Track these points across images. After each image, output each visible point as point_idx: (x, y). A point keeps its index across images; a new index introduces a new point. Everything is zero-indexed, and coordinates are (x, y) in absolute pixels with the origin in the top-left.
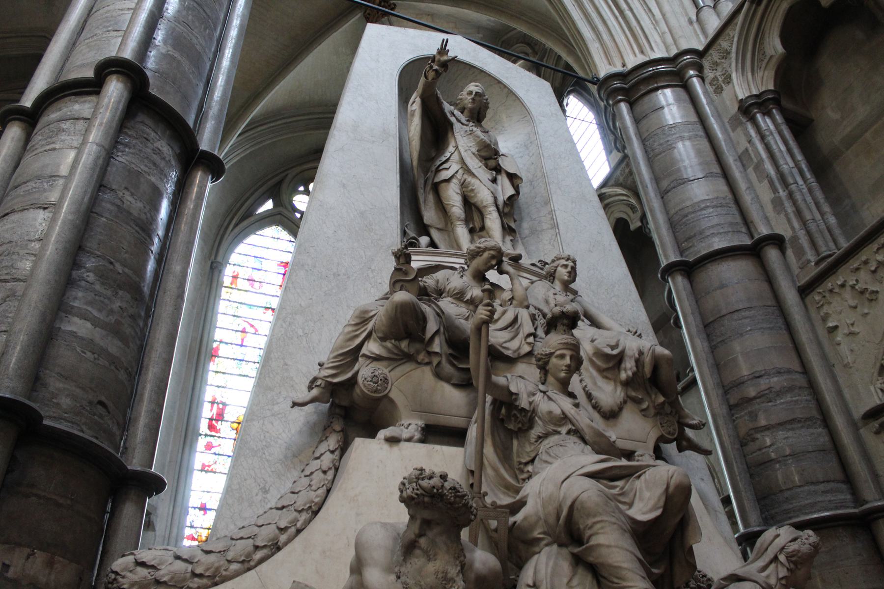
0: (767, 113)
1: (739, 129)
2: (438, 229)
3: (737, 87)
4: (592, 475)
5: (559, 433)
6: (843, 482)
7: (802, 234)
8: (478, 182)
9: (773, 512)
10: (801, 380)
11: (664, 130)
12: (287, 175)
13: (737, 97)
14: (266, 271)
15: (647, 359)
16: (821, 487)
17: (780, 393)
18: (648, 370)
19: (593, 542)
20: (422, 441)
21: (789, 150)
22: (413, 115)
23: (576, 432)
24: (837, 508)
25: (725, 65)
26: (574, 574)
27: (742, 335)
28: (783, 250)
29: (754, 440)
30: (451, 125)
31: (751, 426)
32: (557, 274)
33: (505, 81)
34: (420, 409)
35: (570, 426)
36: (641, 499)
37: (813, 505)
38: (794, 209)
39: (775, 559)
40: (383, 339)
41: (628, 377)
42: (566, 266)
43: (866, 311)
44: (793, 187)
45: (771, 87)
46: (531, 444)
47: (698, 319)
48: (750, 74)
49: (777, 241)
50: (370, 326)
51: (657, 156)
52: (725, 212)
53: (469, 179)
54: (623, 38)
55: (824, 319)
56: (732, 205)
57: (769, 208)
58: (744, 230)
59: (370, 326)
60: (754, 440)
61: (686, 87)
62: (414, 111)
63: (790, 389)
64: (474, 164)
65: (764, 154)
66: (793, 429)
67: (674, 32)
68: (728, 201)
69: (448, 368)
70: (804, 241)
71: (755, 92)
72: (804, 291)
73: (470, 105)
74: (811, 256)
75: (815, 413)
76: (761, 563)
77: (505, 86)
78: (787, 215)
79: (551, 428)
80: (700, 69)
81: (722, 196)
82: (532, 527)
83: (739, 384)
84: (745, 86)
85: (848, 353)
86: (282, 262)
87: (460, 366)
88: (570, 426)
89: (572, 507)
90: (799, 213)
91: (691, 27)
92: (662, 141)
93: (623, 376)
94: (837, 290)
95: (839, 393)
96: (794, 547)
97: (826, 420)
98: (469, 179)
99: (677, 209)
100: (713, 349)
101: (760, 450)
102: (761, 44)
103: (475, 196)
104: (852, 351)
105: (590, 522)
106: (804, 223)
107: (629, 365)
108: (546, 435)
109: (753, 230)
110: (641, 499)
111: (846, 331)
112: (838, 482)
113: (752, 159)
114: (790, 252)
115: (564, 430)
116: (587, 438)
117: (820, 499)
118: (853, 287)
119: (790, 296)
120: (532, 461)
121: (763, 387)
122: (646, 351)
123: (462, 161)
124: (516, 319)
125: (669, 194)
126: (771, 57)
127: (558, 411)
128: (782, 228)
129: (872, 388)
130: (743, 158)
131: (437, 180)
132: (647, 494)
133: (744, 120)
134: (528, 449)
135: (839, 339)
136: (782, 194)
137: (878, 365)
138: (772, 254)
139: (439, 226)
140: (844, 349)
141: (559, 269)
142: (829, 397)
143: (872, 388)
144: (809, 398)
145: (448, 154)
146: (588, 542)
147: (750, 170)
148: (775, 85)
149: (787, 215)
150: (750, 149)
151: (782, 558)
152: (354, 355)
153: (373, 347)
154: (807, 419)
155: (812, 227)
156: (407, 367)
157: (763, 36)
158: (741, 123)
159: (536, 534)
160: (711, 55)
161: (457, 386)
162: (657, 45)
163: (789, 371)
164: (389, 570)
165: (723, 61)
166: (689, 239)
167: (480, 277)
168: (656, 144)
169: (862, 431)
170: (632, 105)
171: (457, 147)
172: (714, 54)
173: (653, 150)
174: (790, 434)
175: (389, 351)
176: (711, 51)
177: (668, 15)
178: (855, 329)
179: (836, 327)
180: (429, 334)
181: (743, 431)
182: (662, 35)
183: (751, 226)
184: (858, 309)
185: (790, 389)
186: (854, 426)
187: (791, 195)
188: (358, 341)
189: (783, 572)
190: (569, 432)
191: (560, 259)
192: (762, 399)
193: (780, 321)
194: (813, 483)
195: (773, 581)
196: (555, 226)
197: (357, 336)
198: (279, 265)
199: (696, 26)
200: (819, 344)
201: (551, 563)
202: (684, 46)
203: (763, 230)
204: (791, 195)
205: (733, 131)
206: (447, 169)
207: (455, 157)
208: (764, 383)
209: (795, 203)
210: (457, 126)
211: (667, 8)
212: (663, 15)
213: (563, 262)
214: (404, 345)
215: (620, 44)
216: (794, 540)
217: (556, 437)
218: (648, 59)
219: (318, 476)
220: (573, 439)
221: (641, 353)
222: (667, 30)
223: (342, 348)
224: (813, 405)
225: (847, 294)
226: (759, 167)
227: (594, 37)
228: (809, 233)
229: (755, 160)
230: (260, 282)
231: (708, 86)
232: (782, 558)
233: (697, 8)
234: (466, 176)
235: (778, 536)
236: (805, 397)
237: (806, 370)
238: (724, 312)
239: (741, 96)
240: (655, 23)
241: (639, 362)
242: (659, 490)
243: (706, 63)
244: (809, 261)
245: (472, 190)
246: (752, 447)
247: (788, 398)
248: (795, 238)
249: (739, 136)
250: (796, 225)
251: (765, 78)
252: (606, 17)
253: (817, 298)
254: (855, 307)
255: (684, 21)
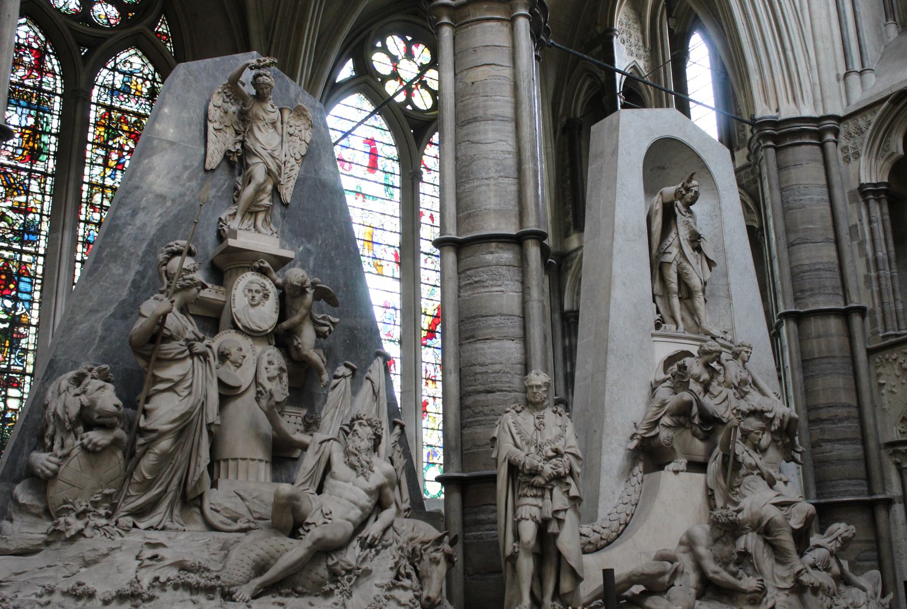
0: (879, 201)
1: (854, 205)
2: (660, 296)
3: (862, 163)
4: (775, 504)
5: (753, 474)
6: (865, 480)
7: (878, 309)
8: (691, 268)
9: (823, 491)
10: (854, 412)
11: (799, 188)
12: (370, 32)
13: (859, 180)
14: (354, 149)
15: (786, 420)
16: (854, 482)
17: (841, 420)
18: (785, 425)
19: (778, 537)
20: (687, 471)
21: (886, 239)
22: (656, 214)
23: (761, 475)
24: (859, 495)
25: (857, 141)
26: (765, 547)
27: (826, 375)
28: (863, 317)
29: (820, 446)
30: (675, 216)
31: (820, 437)
32: (741, 355)
33: (703, 156)
34: (686, 453)
35: (759, 471)
36: (795, 517)
37: (846, 491)
38: (878, 289)
39: (836, 539)
40: (672, 416)
41: (775, 430)
42: (747, 352)
43: (904, 381)
44: (881, 272)
45: (886, 180)
46: (739, 478)
47: (799, 356)
48: (873, 160)
49: (862, 311)
50: (666, 408)
51: (790, 209)
52: (830, 276)
53: (685, 264)
54: (780, 76)
55: (879, 375)
56: (837, 270)
57: (862, 280)
58: (841, 293)
59: (666, 408)
60: (820, 446)
61: (822, 146)
62: (657, 211)
63: (848, 418)
64: (688, 250)
65: (868, 237)
66: (844, 444)
67: (824, 88)
68: (834, 266)
69: (699, 431)
70: (879, 316)
71: (874, 181)
72: (870, 352)
73: (689, 200)
74: (880, 328)
75: (859, 436)
76: (829, 539)
77: (702, 161)
78: (872, 292)
79: (750, 471)
80: (836, 132)
81: (832, 261)
82: (745, 523)
83: (816, 408)
84: (868, 175)
85: (887, 402)
86: (367, 139)
87: (704, 429)
88: (759, 471)
89: (769, 521)
90: (880, 293)
91: (837, 84)
92: (796, 198)
93: (773, 428)
94: (890, 360)
95: (876, 426)
96: (846, 534)
97: (864, 441)
98: (685, 264)
99: (798, 263)
100: (805, 378)
101: (823, 453)
102: (889, 136)
103: (689, 279)
104: (889, 402)
105: (778, 529)
106: (882, 303)
107: (777, 422)
108: (747, 475)
109: (847, 296)
110: (795, 517)
111: (889, 389)
112: (862, 479)
113: (858, 236)
114: (867, 319)
115: (755, 472)
116: (765, 477)
117: (851, 488)
118: (901, 364)
119: (862, 355)
120: (739, 486)
121: (832, 414)
122: (786, 415)
123: (680, 247)
124: (727, 397)
125: (794, 248)
126: (893, 154)
127: (754, 463)
128: (866, 303)
129: (895, 428)
130: (853, 229)
131: (663, 260)
132: (797, 516)
133: (860, 199)
134: (737, 480)
135: (883, 391)
136: (873, 274)
137: (901, 416)
138: (856, 320)
139: (661, 294)
140: (885, 399)
141: (743, 352)
142: (870, 430)
143: (895, 428)
144: (857, 425)
145: (671, 240)
146: (775, 536)
147: (855, 243)
148: (889, 178)
149: (872, 292)
150: (859, 227)
151: (840, 539)
152: (656, 423)
153: (666, 420)
154: (854, 439)
155: (887, 308)
156: (681, 430)
157: (891, 132)
158: (857, 201)
159: (747, 526)
160: (847, 123)
161: (702, 440)
162: (808, 96)
163: (849, 406)
164: (707, 548)
165: (856, 136)
166: (802, 291)
167: (707, 366)
168: (791, 198)
169: (882, 451)
170: (777, 150)
171: (678, 234)
172: (850, 126)
173: (787, 202)
174: (842, 447)
175: (675, 423)
176: (849, 121)
177: (822, 67)
178: (894, 390)
179: (884, 384)
180: (693, 414)
181: (814, 439)
182: (813, 85)
183: (847, 293)
184: (900, 378)
185: (848, 418)
186: (879, 447)
187: (878, 278)
188: (659, 416)
189: (838, 545)
190: (758, 474)
191: (743, 346)
192: (830, 422)
193: (851, 368)
194: (849, 479)
195: (833, 548)
196: (729, 297)
197: (659, 413)
198: (365, 142)
199: (842, 83)
200: (871, 391)
201: (754, 541)
202: (830, 112)
203: (855, 302)
204: (878, 278)
205: (850, 203)
206: (670, 253)
207: (676, 242)
208: (834, 411)
209: (879, 285)
210: (679, 216)
211: (822, 58)
212: (818, 65)
213: (746, 349)
214: (682, 419)
215: (772, 61)
216: (846, 531)
217: (751, 476)
218: (798, 115)
219: (637, 486)
220: (759, 478)
221: (784, 416)
222: (818, 83)
223: (651, 419)
224: (858, 430)
225: (896, 366)
226: (861, 244)
227: (756, 68)
228: (883, 312)
229: (860, 237)
230: (350, 163)
231: (839, 151)
232: (840, 539)
233: (847, 70)
234: (682, 260)
235: (839, 528)
236: (855, 424)
237: (860, 406)
238: (816, 356)
239: (863, 181)
240: (809, 69)
241: (782, 421)
242: (804, 515)
243: (843, 128)
244: (878, 332)
245: (687, 274)
246: (818, 449)
247: (846, 424)
248: (873, 312)
249: (852, 209)
250: (877, 301)
251: (884, 168)
252: (770, 50)
253: (878, 360)
254: (898, 377)
255: (834, 79)
